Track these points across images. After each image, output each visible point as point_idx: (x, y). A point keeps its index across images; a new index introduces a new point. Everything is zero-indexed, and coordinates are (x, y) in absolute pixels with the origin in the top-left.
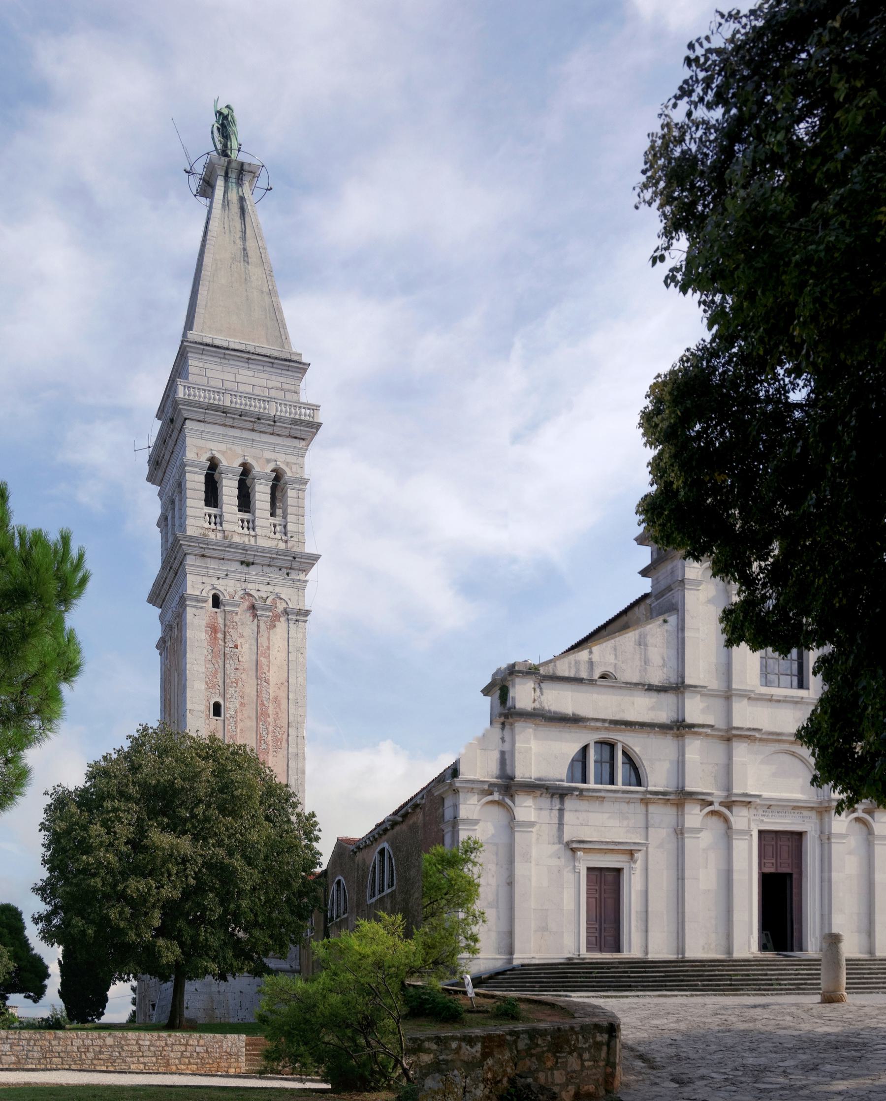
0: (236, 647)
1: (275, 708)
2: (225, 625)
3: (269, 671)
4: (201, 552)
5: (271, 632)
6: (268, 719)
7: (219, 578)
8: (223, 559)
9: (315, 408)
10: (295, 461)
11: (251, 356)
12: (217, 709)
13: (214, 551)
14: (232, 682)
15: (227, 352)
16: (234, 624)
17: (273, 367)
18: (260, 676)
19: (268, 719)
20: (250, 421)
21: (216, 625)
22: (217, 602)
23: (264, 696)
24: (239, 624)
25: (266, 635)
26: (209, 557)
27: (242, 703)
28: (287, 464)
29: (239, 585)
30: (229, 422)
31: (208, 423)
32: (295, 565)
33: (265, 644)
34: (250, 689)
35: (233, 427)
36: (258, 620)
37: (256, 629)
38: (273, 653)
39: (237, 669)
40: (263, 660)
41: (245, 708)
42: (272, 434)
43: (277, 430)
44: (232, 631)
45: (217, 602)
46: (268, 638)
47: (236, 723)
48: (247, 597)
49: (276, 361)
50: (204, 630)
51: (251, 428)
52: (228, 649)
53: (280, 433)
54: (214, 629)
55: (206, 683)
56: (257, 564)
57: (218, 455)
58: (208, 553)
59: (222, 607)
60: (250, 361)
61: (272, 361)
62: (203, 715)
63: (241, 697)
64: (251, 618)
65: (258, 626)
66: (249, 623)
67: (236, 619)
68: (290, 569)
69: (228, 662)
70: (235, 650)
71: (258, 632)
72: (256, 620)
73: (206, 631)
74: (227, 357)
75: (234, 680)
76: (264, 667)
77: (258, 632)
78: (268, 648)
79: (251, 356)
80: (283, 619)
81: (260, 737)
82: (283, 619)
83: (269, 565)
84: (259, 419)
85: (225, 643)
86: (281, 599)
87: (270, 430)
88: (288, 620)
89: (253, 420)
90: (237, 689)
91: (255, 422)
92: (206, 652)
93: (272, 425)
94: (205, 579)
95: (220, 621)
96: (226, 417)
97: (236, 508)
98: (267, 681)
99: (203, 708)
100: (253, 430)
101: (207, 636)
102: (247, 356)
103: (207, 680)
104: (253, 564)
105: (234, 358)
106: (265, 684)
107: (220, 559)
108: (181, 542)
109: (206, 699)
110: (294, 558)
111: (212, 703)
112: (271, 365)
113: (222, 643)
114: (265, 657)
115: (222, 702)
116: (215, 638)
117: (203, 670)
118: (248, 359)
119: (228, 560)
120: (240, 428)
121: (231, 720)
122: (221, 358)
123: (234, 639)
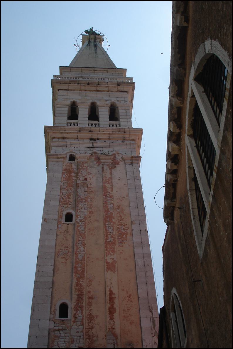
0: (86, 179)
1: (119, 213)
2: (78, 169)
3: (112, 191)
4: (62, 135)
5: (113, 170)
6: (113, 220)
7: (74, 147)
8: (77, 138)
9: (132, 79)
10: (124, 100)
11: (95, 69)
12: (69, 218)
13: (70, 134)
14: (82, 199)
15: (83, 69)
16: (85, 168)
17: (107, 73)
18: (106, 194)
19: (113, 220)
20: (94, 86)
21: (71, 169)
22: (72, 158)
23: (109, 206)
24: (88, 167)
25: (109, 171)
26: (68, 138)
27: (90, 212)
28: (118, 101)
29: (88, 149)
30: (83, 88)
31: (71, 90)
32: (127, 136)
33: (108, 176)
34: (98, 201)
35: (86, 91)
36: (103, 165)
37: (101, 169)
38: (115, 181)
39: (85, 191)
40: (107, 185)
41: (93, 215)
42: (108, 91)
43: (111, 89)
44: (82, 171)
45: (72, 158)
46: (111, 173)
47: (85, 224)
48: (94, 155)
49: (109, 70)
50: (61, 172)
51: (96, 90)
52: (79, 181)
53: (112, 90)
54: (68, 171)
55: (60, 201)
56: (100, 139)
57: (76, 100)
58: (66, 135)
59: (76, 160)
60: (95, 71)
61: (106, 70)
62: (57, 221)
63: (90, 208)
64: (97, 164)
65: (103, 168)
66: (96, 167)
67: (86, 165)
68: (124, 139)
69: (79, 188)
70: (86, 181)
71: (103, 171)
72: (101, 166)
73: (63, 173)
74: (83, 71)
75: (83, 198)
76: (108, 189)
77: (103, 171)
78: (111, 178)
79: (95, 69)
80: (121, 164)
81: (107, 233)
82: (121, 164)
83: (109, 139)
84: (98, 84)
85: (77, 178)
86: (118, 154)
87: (106, 89)
88: (125, 163)
89: (96, 85)
90: (86, 203)
91: (97, 86)
92: (62, 184)
93: (107, 87)
94: (64, 148)
95: (74, 167)
96: (81, 86)
97: (87, 119)
98: (111, 197)
99: (56, 217)
100: (97, 91)
101: (64, 176)
102: (93, 69)
103: (61, 199)
104: (98, 139)
105: (86, 71)
106: (109, 198)
107: (75, 139)
108: (48, 131)
109: (60, 212)
110: (125, 132)
111: (65, 213)
112: (106, 72)
113: (73, 178)
114: (109, 183)
115: (73, 213)
116: (70, 176)
117: (59, 193)
118: (94, 71)
119: (81, 138)
120: (90, 91)
121: (80, 223)
122: (80, 72)
123: (84, 175)
